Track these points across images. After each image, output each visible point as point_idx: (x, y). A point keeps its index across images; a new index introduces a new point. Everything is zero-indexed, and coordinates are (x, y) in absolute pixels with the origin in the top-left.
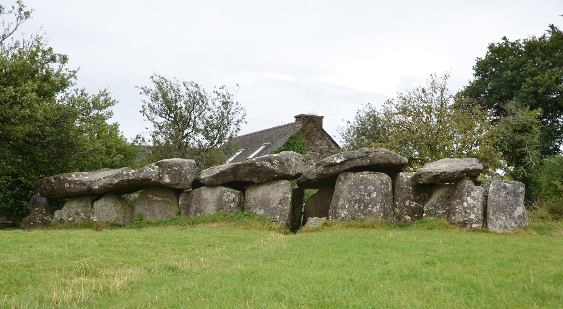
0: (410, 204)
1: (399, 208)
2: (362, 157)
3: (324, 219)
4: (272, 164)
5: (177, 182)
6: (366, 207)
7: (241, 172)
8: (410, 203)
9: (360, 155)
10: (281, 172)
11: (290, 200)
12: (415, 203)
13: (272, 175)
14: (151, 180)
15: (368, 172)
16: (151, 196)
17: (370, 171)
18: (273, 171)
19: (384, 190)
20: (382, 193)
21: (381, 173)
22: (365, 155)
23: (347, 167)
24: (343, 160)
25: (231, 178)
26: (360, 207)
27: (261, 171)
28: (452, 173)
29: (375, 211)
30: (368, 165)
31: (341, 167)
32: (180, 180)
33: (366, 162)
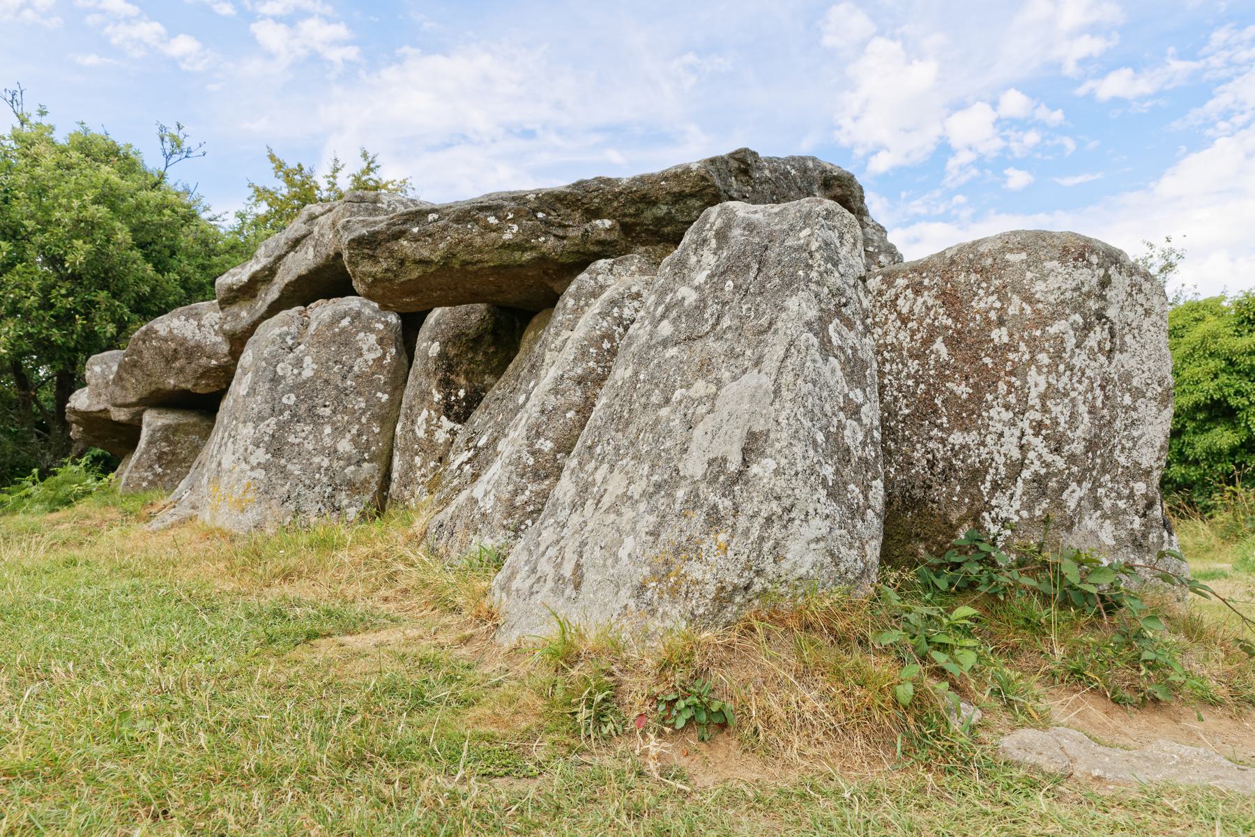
0: (430, 433)
1: (404, 451)
4: (200, 326)
5: (102, 407)
13: (204, 361)
19: (299, 363)
20: (275, 380)
31: (264, 301)
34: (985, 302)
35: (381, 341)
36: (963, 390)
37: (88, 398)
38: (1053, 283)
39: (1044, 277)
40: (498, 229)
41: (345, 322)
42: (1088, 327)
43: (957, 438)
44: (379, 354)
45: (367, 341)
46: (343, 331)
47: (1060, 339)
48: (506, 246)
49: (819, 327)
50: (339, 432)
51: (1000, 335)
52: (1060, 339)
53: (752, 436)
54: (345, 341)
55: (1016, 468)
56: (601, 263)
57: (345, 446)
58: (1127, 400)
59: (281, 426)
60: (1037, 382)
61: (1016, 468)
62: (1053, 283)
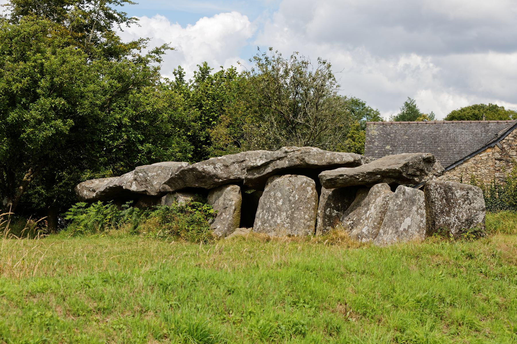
0: (331, 213)
2: (281, 158)
3: (250, 229)
4: (215, 168)
6: (273, 217)
7: (189, 177)
8: (330, 211)
9: (279, 156)
10: (225, 176)
11: (234, 208)
12: (335, 211)
13: (216, 180)
14: (122, 187)
15: (290, 175)
16: (142, 203)
17: (292, 174)
18: (216, 176)
19: (294, 197)
20: (290, 201)
21: (299, 176)
22: (284, 155)
23: (269, 170)
24: (264, 162)
25: (180, 185)
26: (268, 216)
27: (204, 177)
28: (351, 176)
29: (279, 221)
30: (287, 167)
31: (264, 171)
32: (147, 187)
33: (284, 164)
34: (450, 194)
35: (312, 189)
36: (448, 209)
37: (136, 186)
38: (459, 194)
39: (457, 193)
40: (359, 179)
41: (304, 185)
42: (465, 201)
43: (447, 218)
44: (312, 192)
45: (309, 188)
46: (304, 187)
47: (460, 203)
48: (360, 181)
49: (417, 211)
50: (305, 213)
51: (452, 201)
52: (460, 203)
53: (409, 226)
54: (304, 190)
55: (454, 223)
56: (380, 185)
57: (306, 216)
58: (475, 211)
59: (293, 213)
60: (456, 210)
61: (454, 223)
62: (459, 194)
